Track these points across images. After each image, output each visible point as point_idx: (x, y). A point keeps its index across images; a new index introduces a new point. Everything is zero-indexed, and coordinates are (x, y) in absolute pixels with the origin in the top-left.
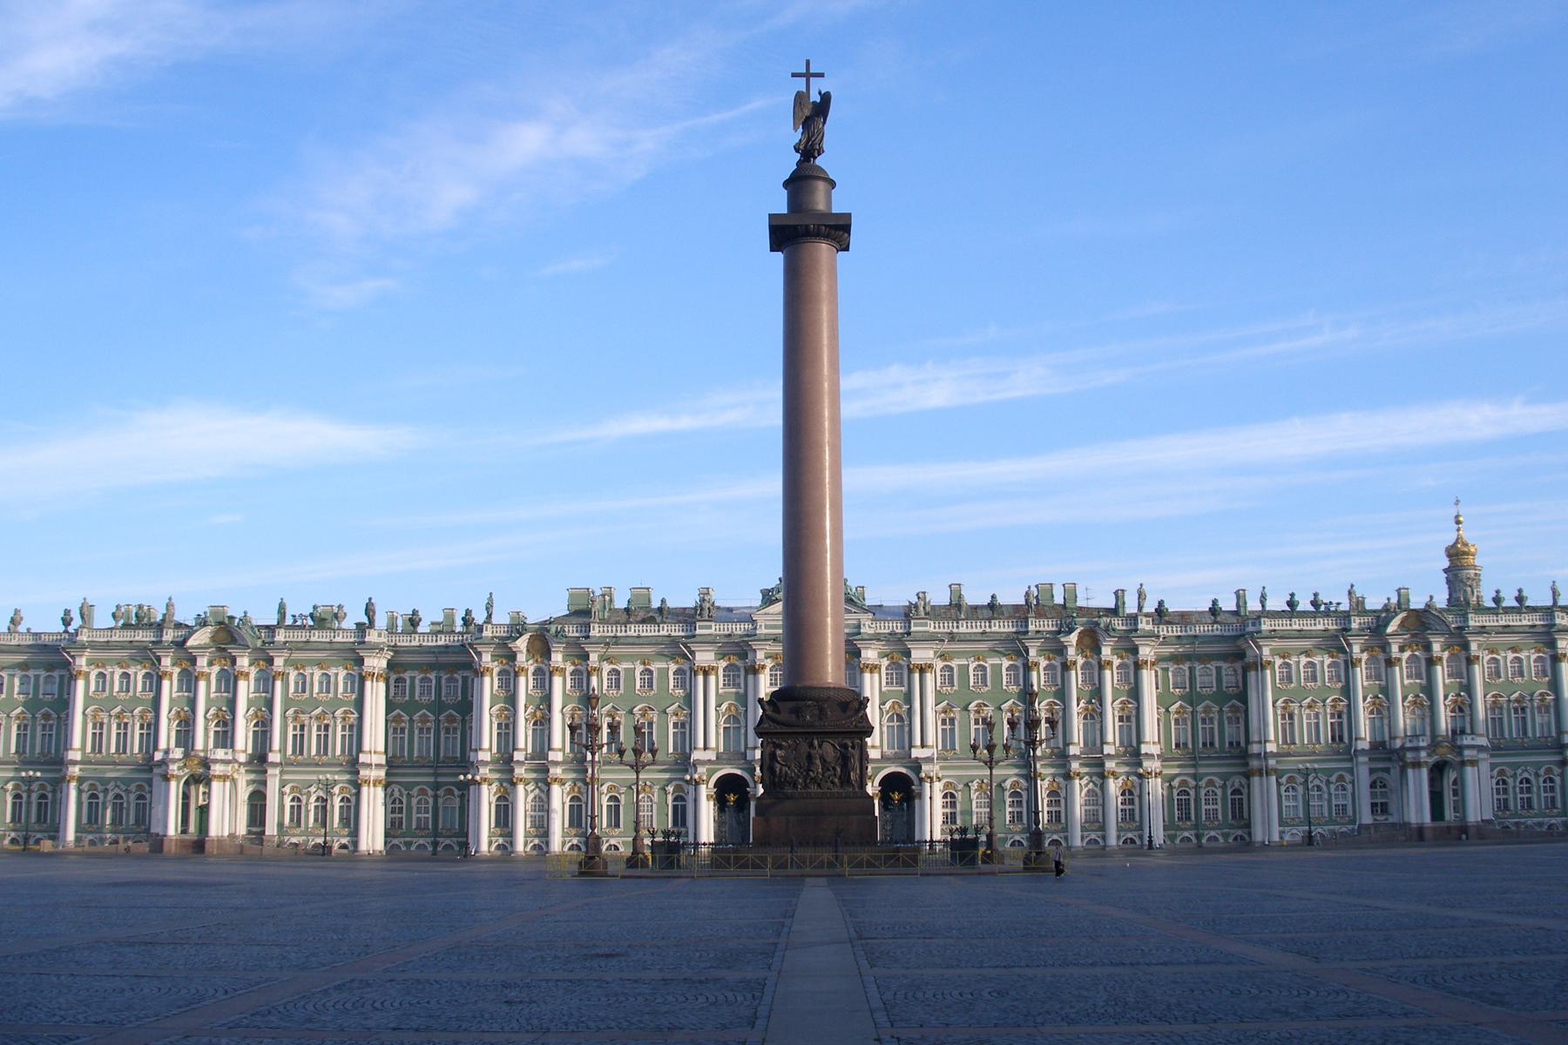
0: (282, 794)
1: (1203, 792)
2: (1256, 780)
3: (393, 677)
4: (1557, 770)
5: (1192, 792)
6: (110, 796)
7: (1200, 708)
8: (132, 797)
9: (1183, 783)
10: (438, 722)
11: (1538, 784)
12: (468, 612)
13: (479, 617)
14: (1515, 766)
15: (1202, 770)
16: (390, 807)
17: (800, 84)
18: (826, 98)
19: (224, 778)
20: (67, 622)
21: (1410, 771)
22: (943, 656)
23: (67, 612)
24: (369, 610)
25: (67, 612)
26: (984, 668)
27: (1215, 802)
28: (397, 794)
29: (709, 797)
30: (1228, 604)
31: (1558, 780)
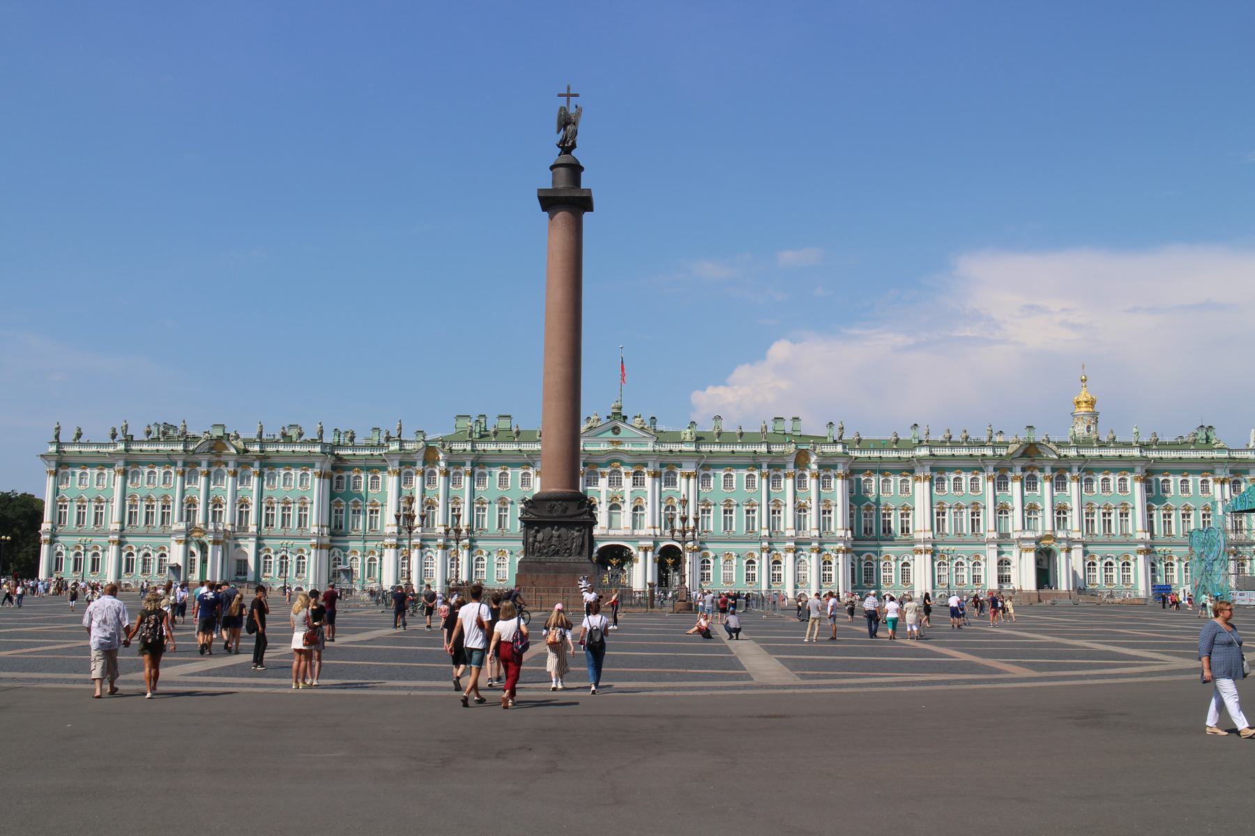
2: (917, 557)
9: (869, 557)
11: (1117, 565)
13: (394, 434)
20: (114, 436)
22: (706, 467)
31: (1132, 563)
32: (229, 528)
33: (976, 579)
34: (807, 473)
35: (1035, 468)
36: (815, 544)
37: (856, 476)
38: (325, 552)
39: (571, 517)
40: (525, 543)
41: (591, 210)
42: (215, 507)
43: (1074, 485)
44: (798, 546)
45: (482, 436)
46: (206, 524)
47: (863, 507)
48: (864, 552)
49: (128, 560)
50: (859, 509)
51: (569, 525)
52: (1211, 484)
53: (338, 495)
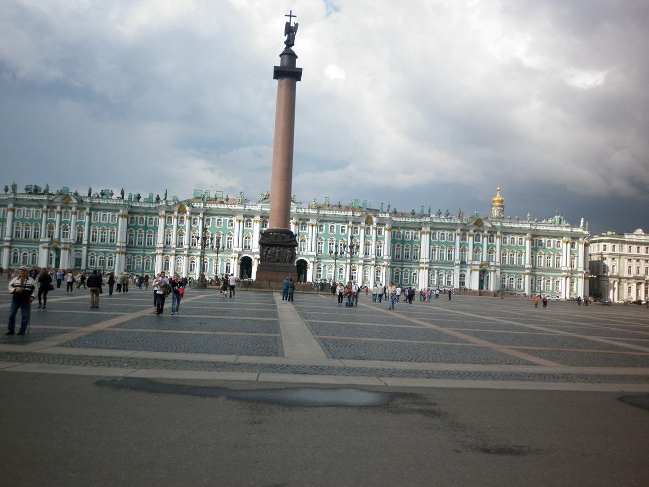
0: (87, 256)
1: (403, 273)
2: (421, 271)
3: (130, 217)
4: (523, 276)
5: (400, 273)
6: (22, 254)
7: (405, 246)
8: (31, 254)
9: (397, 270)
10: (145, 233)
12: (158, 196)
13: (162, 197)
14: (509, 274)
15: (404, 266)
16: (127, 262)
17: (287, 19)
18: (297, 25)
19: (65, 249)
20: (6, 190)
21: (473, 272)
23: (7, 187)
24: (123, 193)
25: (7, 187)
26: (334, 226)
27: (407, 277)
28: (129, 257)
29: (238, 264)
30: (418, 211)
32: (72, 242)
33: (449, 283)
34: (371, 227)
35: (480, 231)
36: (373, 262)
37: (394, 230)
38: (123, 256)
39: (287, 242)
40: (261, 255)
41: (300, 80)
42: (64, 230)
43: (498, 240)
44: (366, 263)
45: (207, 201)
46: (59, 239)
47: (396, 245)
48: (395, 267)
49: (14, 257)
50: (394, 246)
51: (285, 246)
52: (561, 243)
53: (132, 227)
